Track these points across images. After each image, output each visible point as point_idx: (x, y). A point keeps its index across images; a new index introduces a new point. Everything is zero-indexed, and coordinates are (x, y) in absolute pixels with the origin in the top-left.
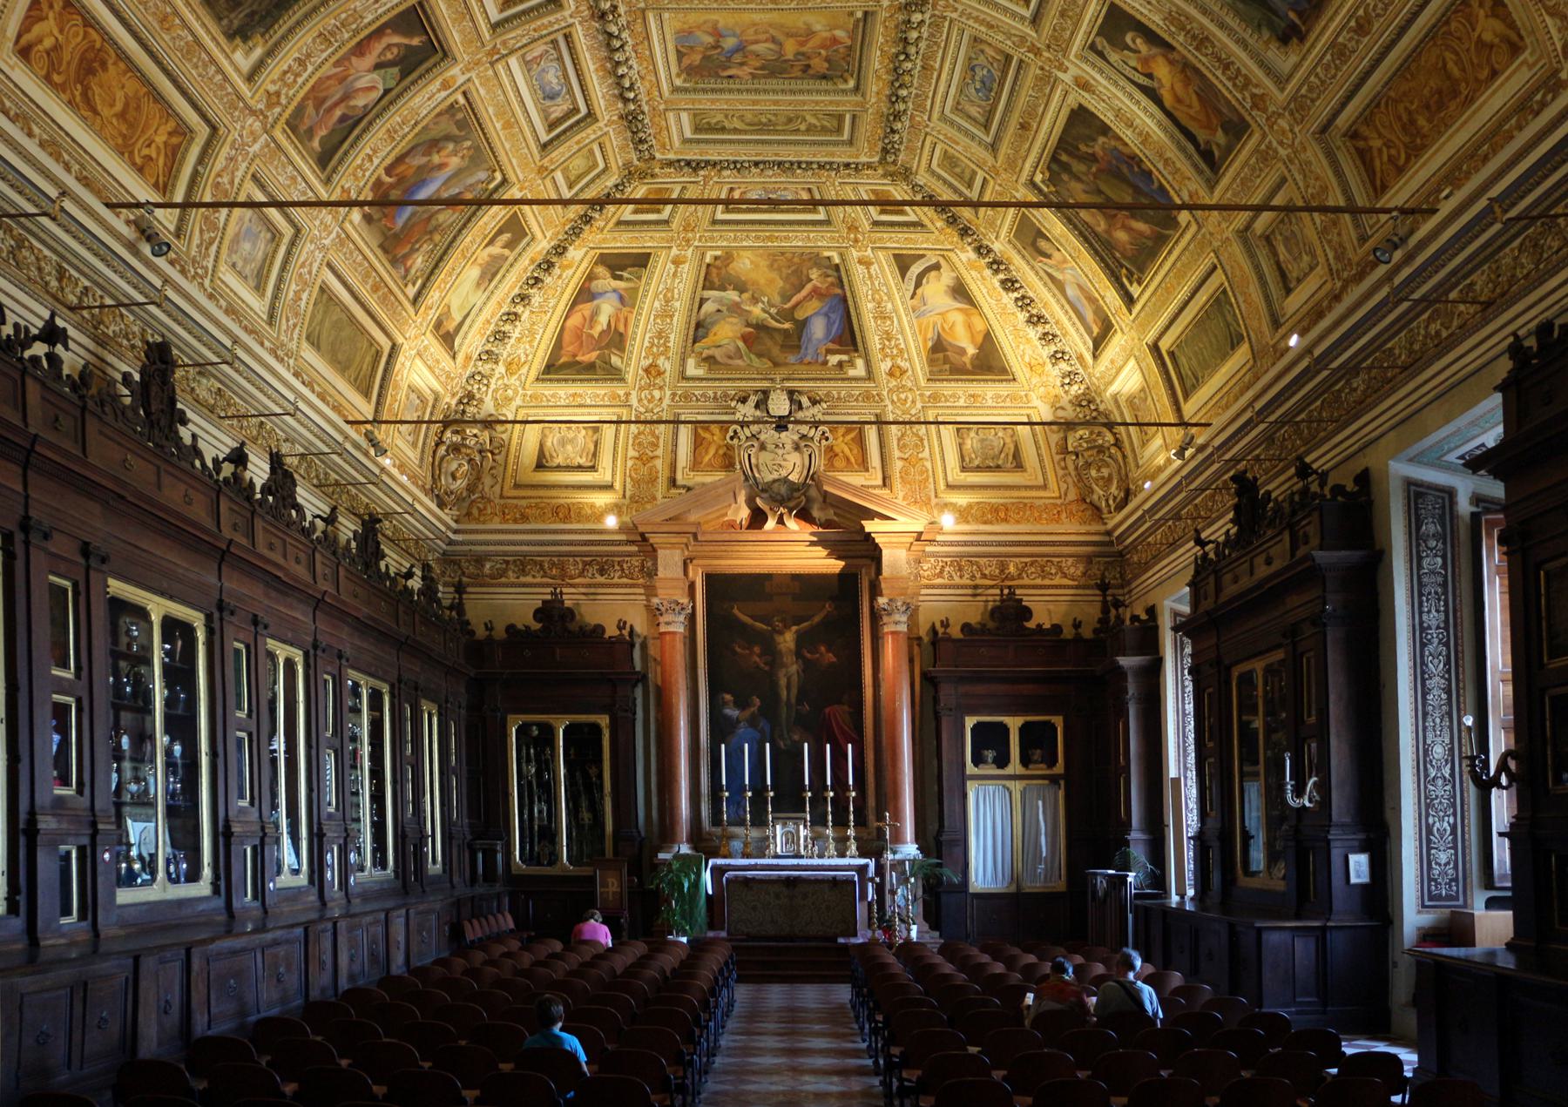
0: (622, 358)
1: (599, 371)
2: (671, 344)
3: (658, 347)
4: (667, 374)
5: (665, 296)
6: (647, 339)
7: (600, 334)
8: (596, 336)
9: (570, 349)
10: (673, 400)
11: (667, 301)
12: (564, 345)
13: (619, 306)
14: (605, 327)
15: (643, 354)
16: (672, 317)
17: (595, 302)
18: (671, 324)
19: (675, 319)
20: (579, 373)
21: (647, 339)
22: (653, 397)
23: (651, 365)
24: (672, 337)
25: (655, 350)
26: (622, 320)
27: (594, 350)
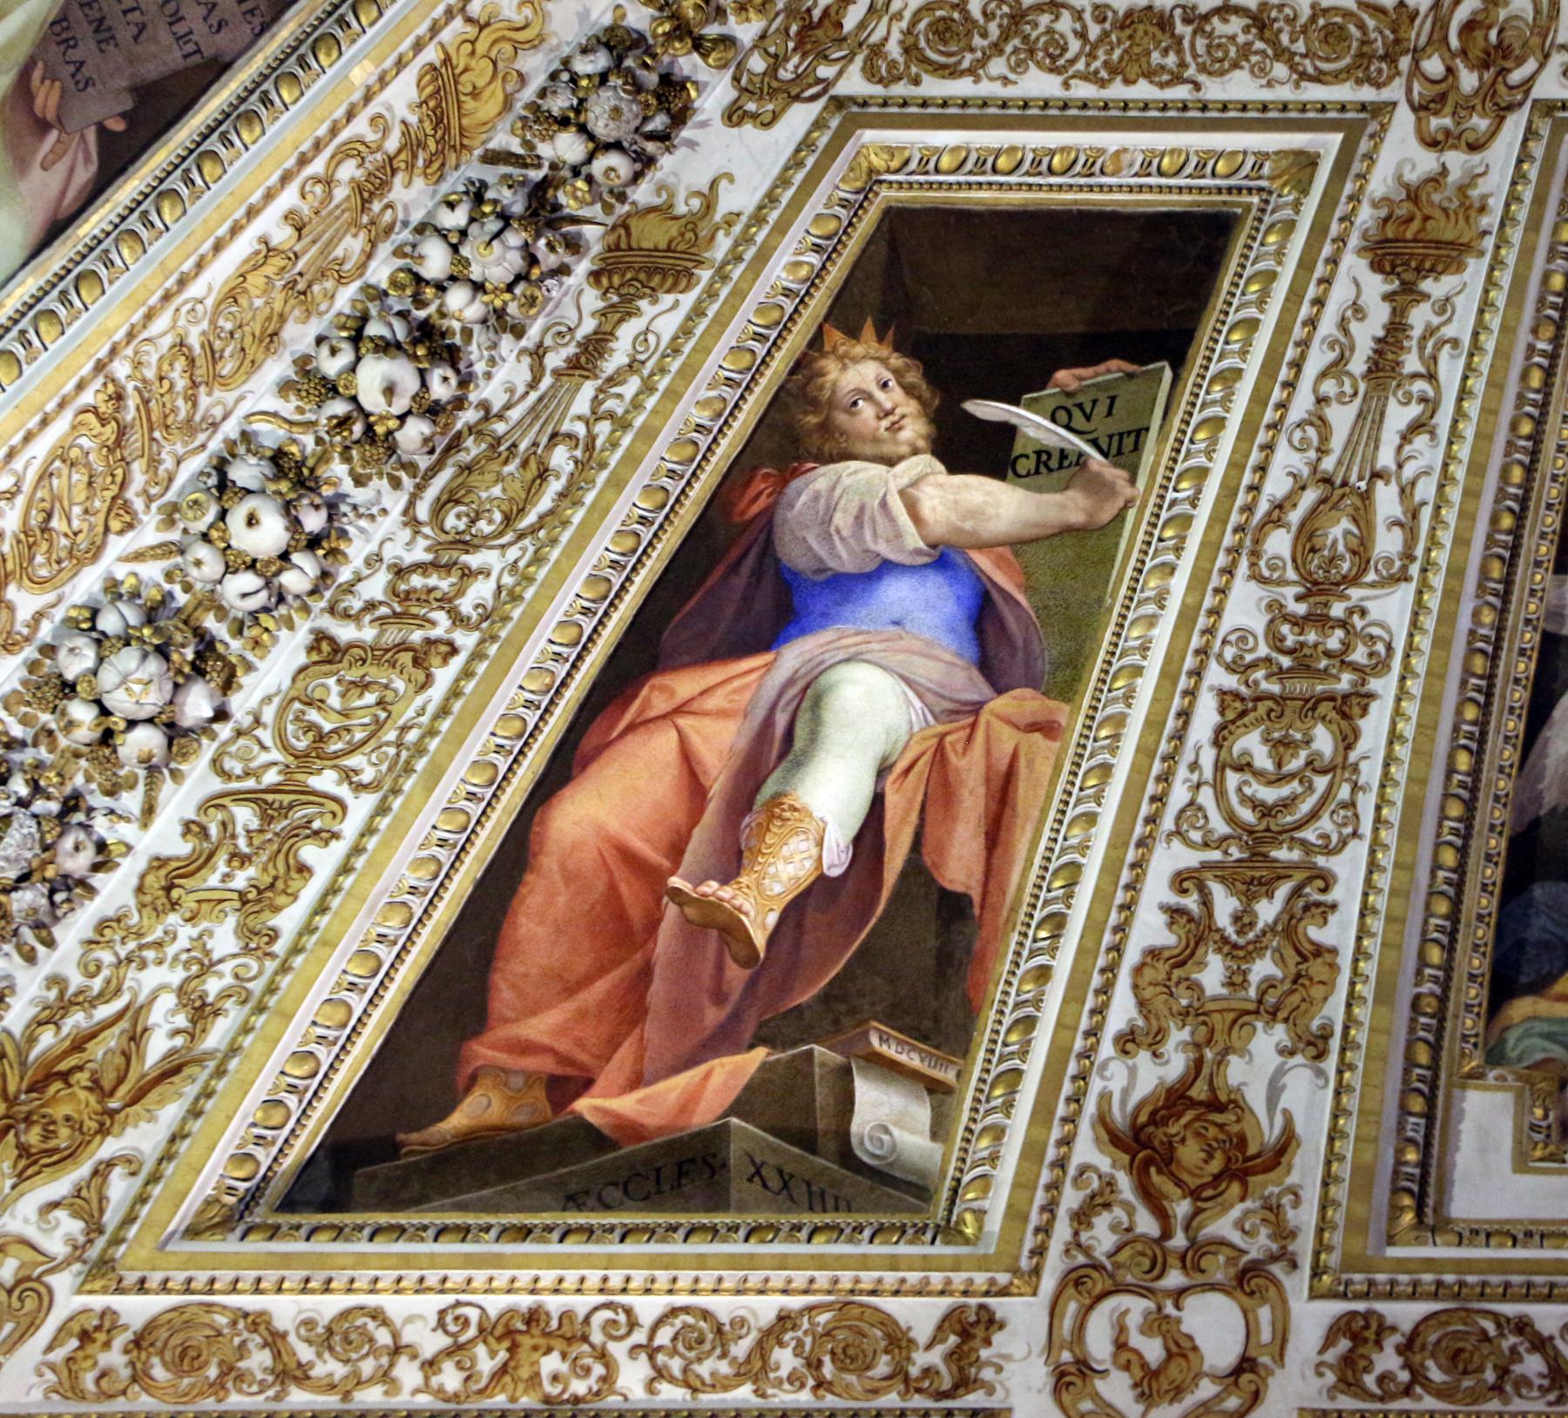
0: (935, 1088)
1: (739, 1187)
2: (1337, 932)
3: (1239, 953)
4: (1306, 1169)
5: (1307, 539)
6: (1156, 890)
7: (796, 911)
8: (760, 925)
9: (539, 1028)
10: (1349, 1373)
11: (1318, 588)
12: (503, 996)
13: (966, 682)
14: (836, 859)
15: (1122, 1011)
16: (1350, 708)
17: (793, 656)
18: (1341, 766)
19: (1374, 727)
20: (574, 1201)
21: (1156, 890)
22: (1181, 1349)
23: (1174, 1099)
24: (1348, 868)
25: (1212, 974)
26: (972, 803)
27: (723, 1041)
